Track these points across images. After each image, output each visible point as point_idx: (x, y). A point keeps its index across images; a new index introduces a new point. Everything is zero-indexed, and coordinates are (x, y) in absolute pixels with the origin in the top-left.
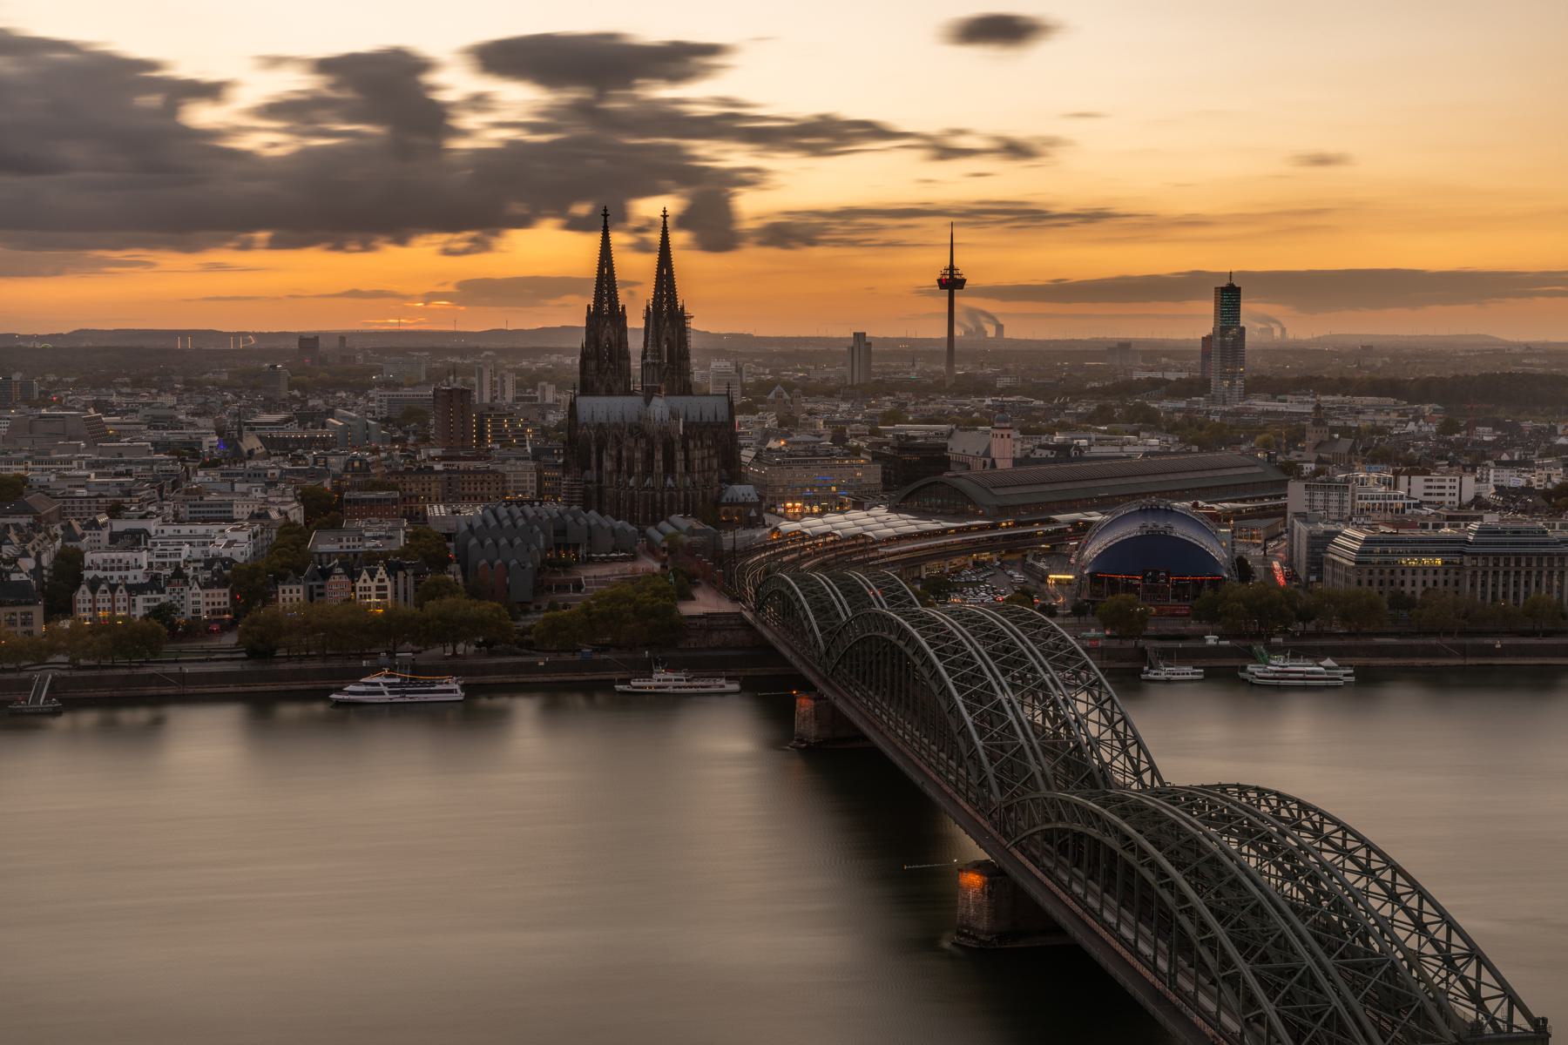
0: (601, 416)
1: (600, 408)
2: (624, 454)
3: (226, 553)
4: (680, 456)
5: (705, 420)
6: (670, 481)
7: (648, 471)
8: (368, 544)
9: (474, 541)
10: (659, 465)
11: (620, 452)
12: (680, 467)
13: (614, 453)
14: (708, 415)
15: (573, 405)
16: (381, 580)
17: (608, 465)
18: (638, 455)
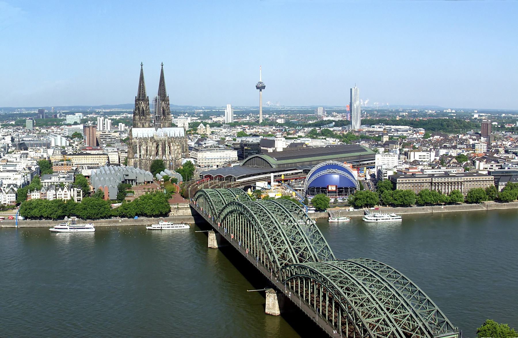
0: (140, 135)
1: (138, 132)
2: (148, 148)
3: (14, 182)
4: (167, 149)
5: (176, 136)
6: (164, 157)
7: (157, 154)
8: (61, 179)
9: (97, 178)
10: (160, 152)
11: (147, 148)
12: (167, 152)
13: (145, 148)
14: (177, 135)
15: (131, 131)
16: (65, 192)
17: (143, 152)
18: (153, 149)
